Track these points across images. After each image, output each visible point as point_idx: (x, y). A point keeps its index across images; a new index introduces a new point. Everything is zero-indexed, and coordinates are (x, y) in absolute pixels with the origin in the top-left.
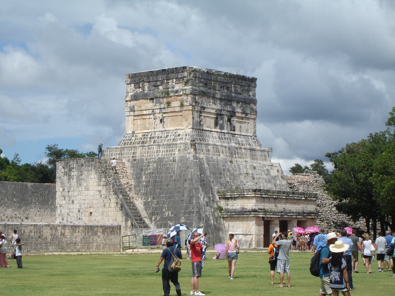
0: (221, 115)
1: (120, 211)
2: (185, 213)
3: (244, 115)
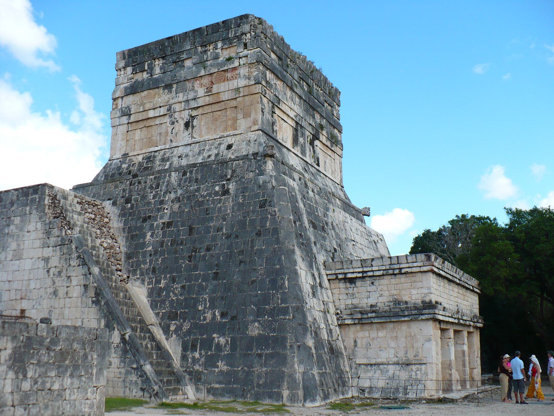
1: (94, 306)
2: (259, 313)
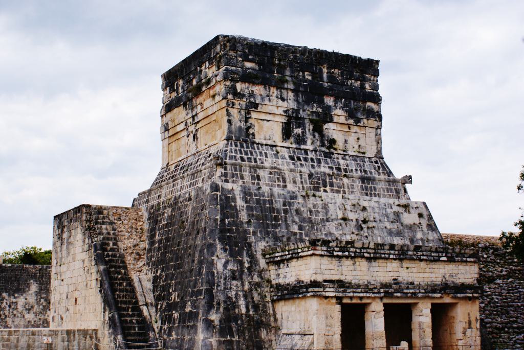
3: (351, 121)
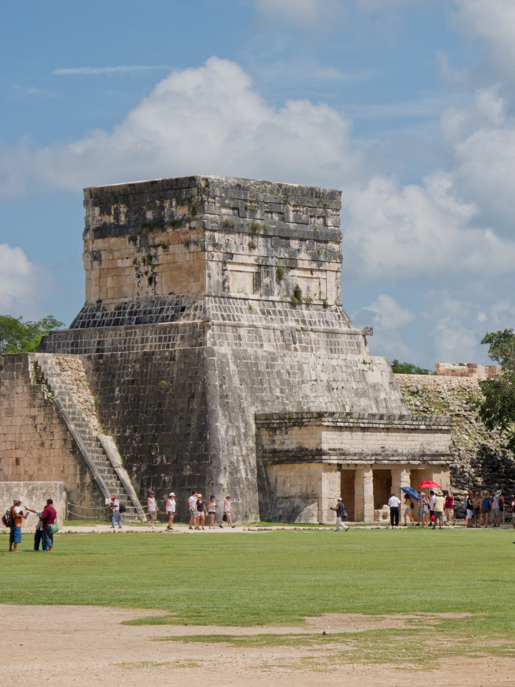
0: (267, 266)
1: (71, 455)
2: (191, 460)
3: (314, 266)
